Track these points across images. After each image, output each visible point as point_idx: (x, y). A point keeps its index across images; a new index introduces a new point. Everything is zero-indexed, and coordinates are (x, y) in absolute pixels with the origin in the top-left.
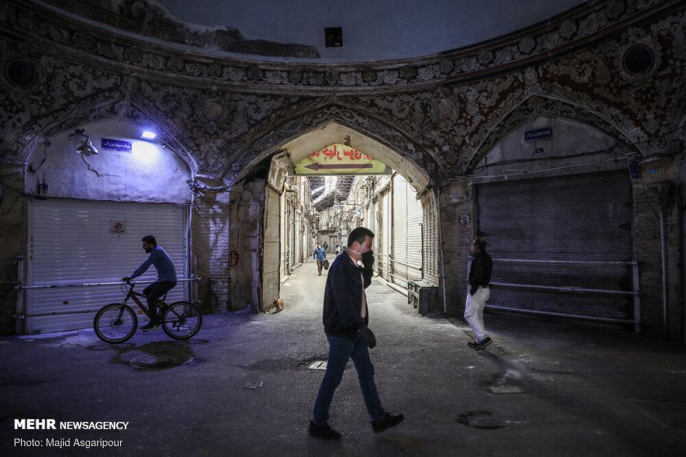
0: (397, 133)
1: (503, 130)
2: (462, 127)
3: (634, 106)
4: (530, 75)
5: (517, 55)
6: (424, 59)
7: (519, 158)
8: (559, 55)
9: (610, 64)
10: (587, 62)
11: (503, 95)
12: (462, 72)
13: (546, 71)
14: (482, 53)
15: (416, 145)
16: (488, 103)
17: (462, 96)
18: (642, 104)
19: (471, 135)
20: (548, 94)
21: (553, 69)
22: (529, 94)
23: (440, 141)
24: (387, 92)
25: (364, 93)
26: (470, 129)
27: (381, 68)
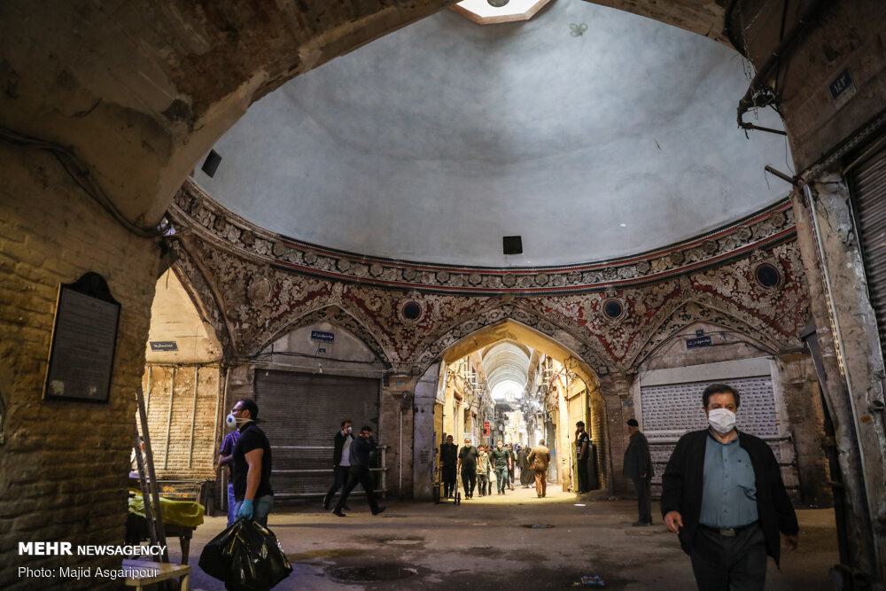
0: (211, 295)
1: (301, 323)
2: (268, 311)
3: (398, 338)
4: (338, 288)
5: (334, 268)
6: (264, 233)
7: (306, 353)
8: (363, 284)
9: (394, 307)
10: (380, 298)
11: (311, 296)
12: (288, 260)
13: (349, 291)
14: (311, 254)
15: (221, 314)
16: (297, 297)
17: (280, 282)
18: (404, 338)
19: (273, 320)
20: (346, 308)
21: (354, 291)
22: (330, 302)
23: (244, 317)
24: (227, 249)
25: (210, 241)
26: (275, 314)
27: (231, 221)
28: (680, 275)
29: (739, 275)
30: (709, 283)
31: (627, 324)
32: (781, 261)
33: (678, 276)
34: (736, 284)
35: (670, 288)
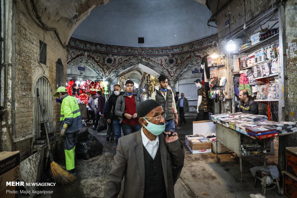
3: (105, 70)
5: (85, 47)
10: (99, 57)
16: (73, 56)
28: (191, 52)
30: (199, 55)
31: (175, 66)
35: (188, 56)
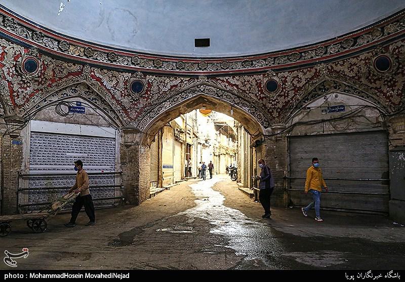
28: (86, 63)
29: (121, 79)
30: (101, 77)
32: (149, 83)
33: (84, 64)
34: (117, 84)
